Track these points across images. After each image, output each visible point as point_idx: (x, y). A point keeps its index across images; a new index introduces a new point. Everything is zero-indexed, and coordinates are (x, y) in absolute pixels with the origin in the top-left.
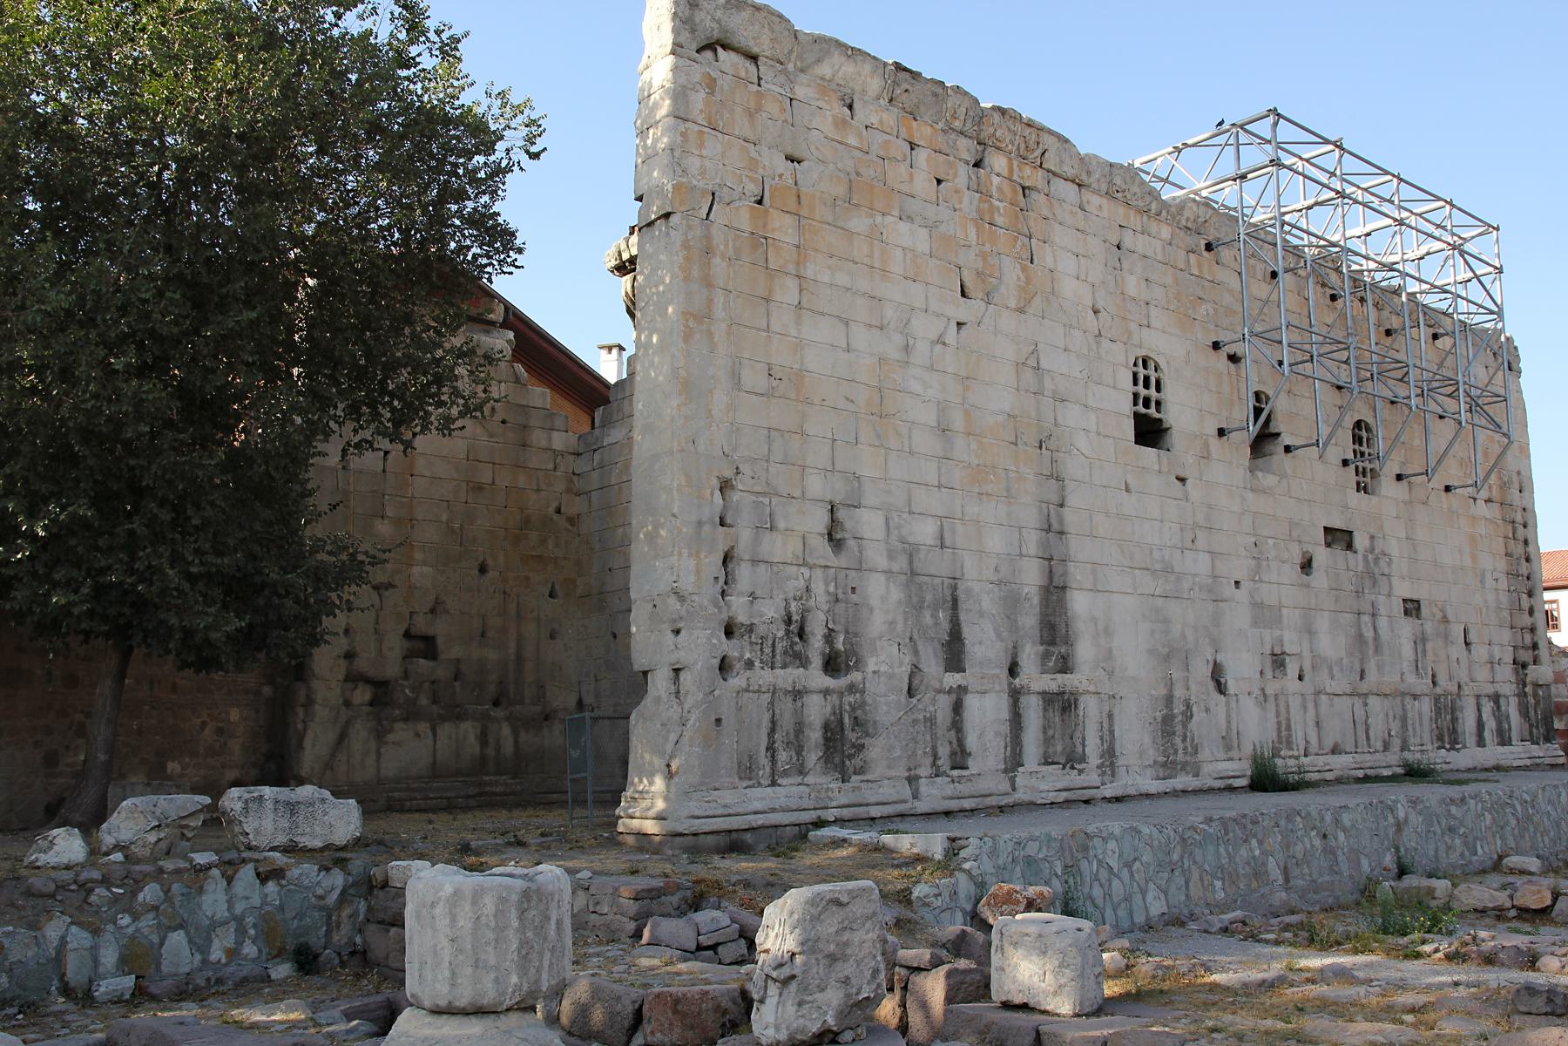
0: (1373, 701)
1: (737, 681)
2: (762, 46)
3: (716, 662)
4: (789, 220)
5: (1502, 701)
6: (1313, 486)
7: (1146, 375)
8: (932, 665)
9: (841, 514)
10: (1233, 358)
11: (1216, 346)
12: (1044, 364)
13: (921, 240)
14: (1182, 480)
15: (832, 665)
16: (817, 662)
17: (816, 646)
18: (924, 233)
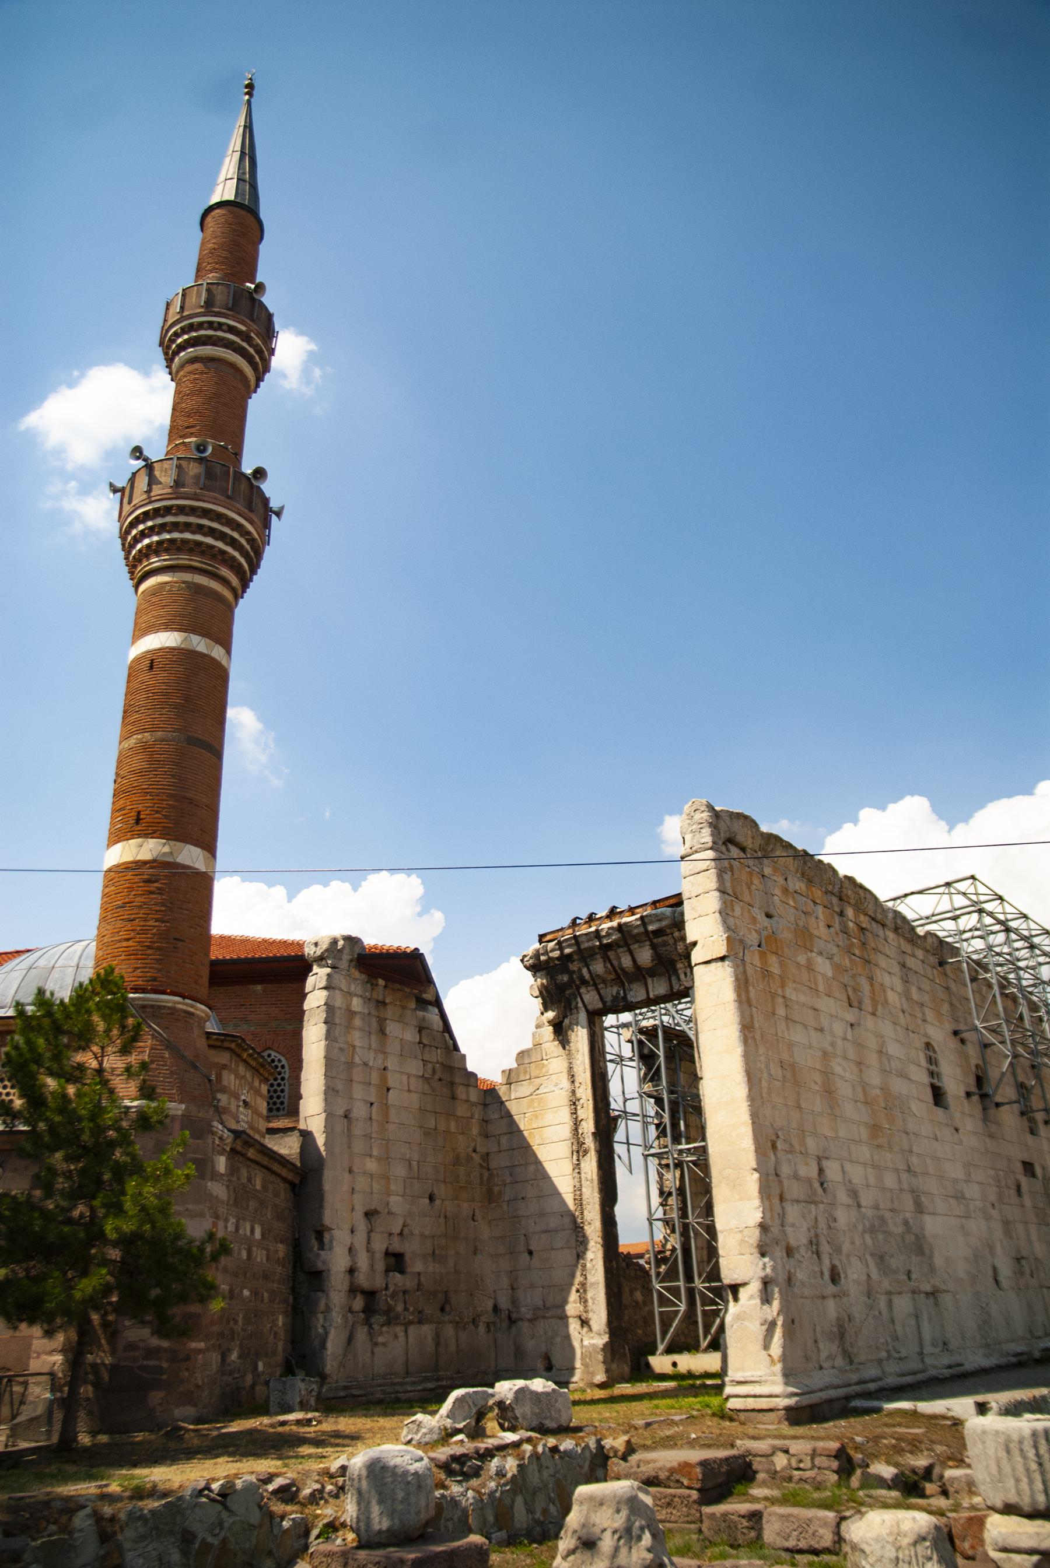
2: (749, 843)
9: (825, 1163)
10: (963, 1041)
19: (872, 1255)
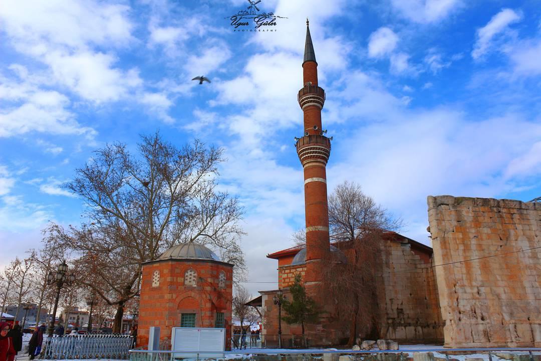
1: (463, 321)
17: (479, 315)
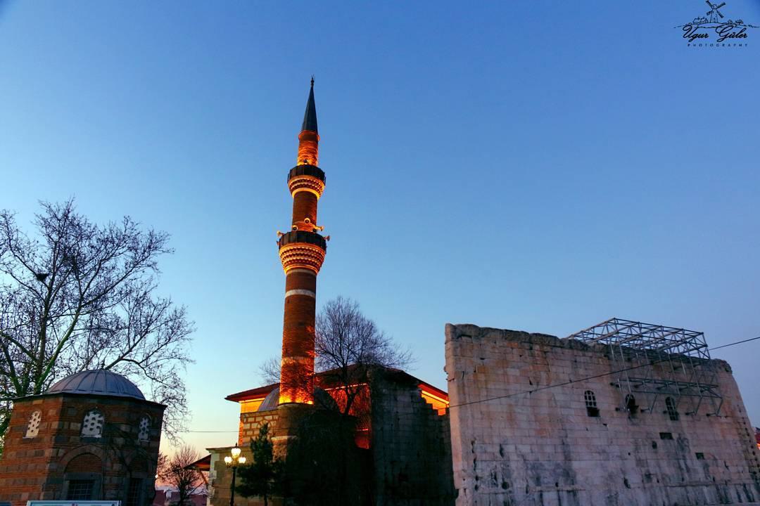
0: (689, 488)
1: (480, 491)
2: (473, 334)
3: (474, 487)
4: (483, 375)
5: (747, 486)
6: (655, 422)
7: (589, 396)
8: (532, 484)
9: (503, 446)
11: (612, 384)
12: (557, 398)
13: (517, 372)
14: (605, 425)
15: (505, 486)
16: (500, 486)
17: (500, 481)
18: (518, 370)
19: (531, 478)
